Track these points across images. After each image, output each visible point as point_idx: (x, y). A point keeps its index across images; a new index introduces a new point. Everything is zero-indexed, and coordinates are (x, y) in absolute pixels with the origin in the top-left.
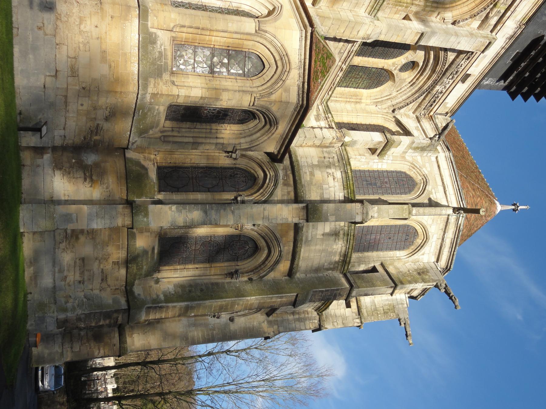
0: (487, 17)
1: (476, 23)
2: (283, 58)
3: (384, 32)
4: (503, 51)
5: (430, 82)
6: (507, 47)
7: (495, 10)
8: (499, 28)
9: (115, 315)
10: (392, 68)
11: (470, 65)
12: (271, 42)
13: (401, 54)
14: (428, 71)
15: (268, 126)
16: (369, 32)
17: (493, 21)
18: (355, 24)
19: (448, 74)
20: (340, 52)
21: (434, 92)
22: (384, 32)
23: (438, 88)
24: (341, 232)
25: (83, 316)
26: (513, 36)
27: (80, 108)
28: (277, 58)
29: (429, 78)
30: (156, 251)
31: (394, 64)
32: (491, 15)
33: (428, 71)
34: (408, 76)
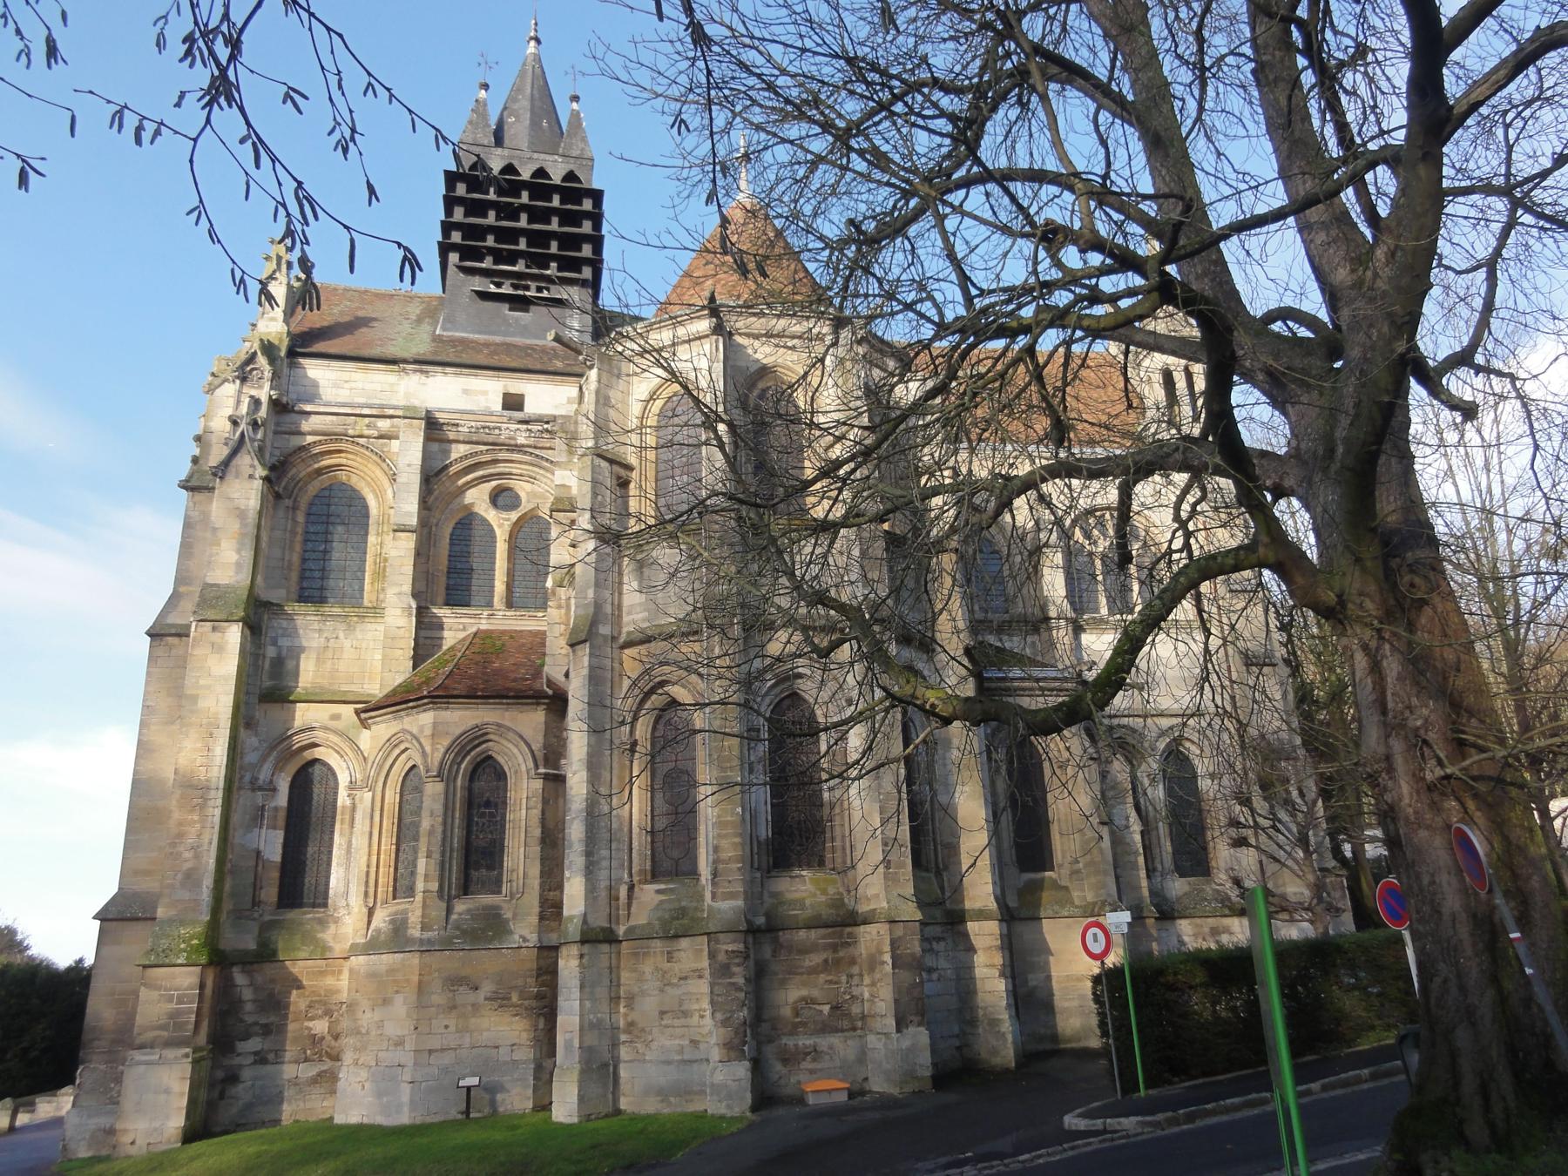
0: (381, 437)
1: (395, 445)
2: (392, 743)
3: (396, 590)
4: (448, 370)
5: (516, 456)
6: (439, 369)
7: (366, 432)
8: (391, 412)
9: (722, 957)
10: (507, 526)
11: (465, 417)
12: (381, 767)
13: (485, 522)
14: (501, 468)
15: (491, 737)
16: (399, 612)
17: (384, 424)
18: (390, 640)
19: (491, 439)
20: (464, 629)
21: (531, 441)
22: (396, 590)
23: (521, 440)
24: (639, 557)
25: (719, 1016)
26: (422, 372)
27: (452, 1029)
28: (397, 751)
29: (512, 461)
30: (663, 886)
31: (501, 526)
32: (376, 434)
33: (501, 468)
34: (522, 488)
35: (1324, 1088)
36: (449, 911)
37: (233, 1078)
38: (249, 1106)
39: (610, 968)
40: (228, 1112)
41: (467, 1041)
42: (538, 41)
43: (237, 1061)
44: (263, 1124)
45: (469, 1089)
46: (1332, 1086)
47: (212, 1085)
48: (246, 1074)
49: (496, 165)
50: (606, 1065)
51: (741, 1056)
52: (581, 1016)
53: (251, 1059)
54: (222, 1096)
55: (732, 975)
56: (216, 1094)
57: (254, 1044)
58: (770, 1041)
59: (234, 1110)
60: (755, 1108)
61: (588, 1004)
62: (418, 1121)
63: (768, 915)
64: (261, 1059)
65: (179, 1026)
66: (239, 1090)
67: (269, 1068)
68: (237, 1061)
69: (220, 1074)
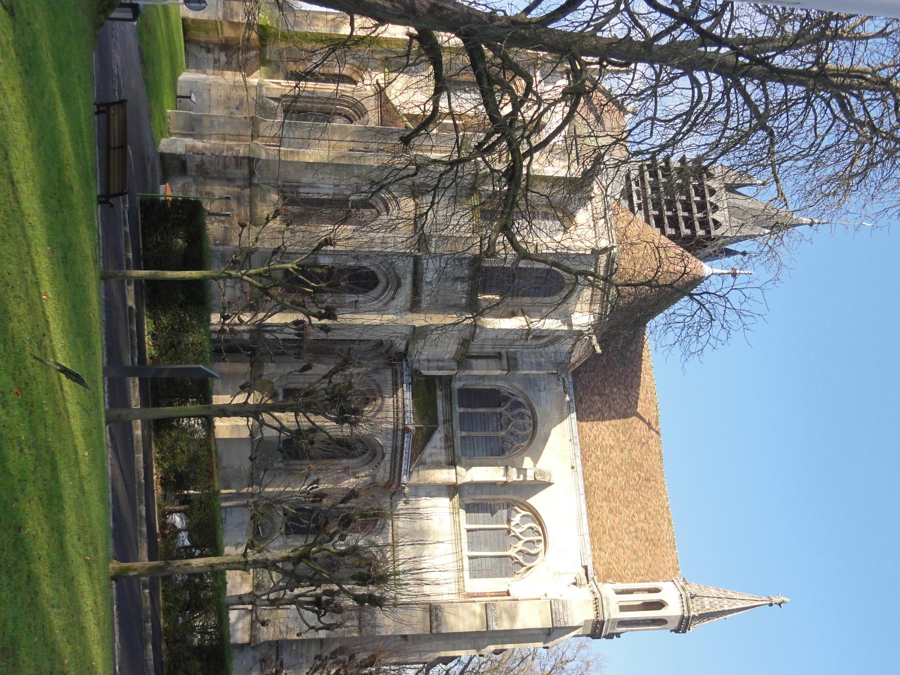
35: (125, 232)
36: (275, 99)
37: (209, 51)
38: (196, 57)
39: (239, 135)
40: (194, 49)
41: (213, 104)
42: (811, 225)
43: (216, 52)
44: (187, 62)
45: (190, 97)
46: (126, 236)
47: (207, 43)
48: (210, 56)
49: (714, 184)
50: (193, 130)
51: (187, 151)
52: (217, 116)
53: (216, 57)
54: (201, 47)
55: (227, 151)
56: (203, 45)
57: (223, 58)
58: (194, 181)
59: (195, 52)
60: (163, 156)
61: (222, 120)
62: (179, 84)
63: (257, 185)
64: (216, 61)
65: (232, 16)
66: (203, 53)
67: (212, 64)
68: (216, 52)
69: (211, 46)
